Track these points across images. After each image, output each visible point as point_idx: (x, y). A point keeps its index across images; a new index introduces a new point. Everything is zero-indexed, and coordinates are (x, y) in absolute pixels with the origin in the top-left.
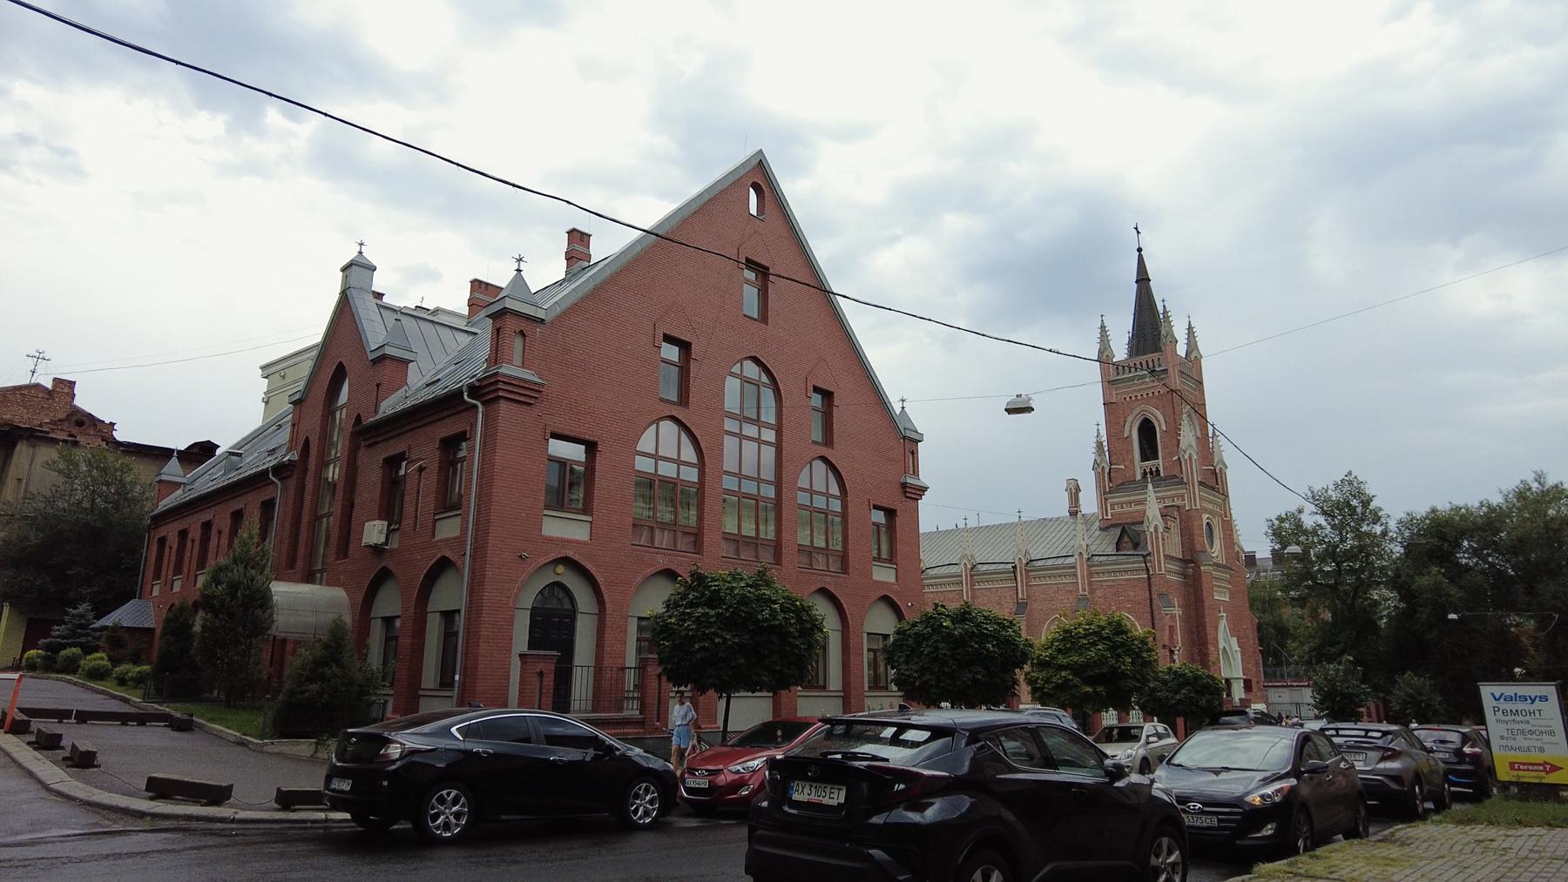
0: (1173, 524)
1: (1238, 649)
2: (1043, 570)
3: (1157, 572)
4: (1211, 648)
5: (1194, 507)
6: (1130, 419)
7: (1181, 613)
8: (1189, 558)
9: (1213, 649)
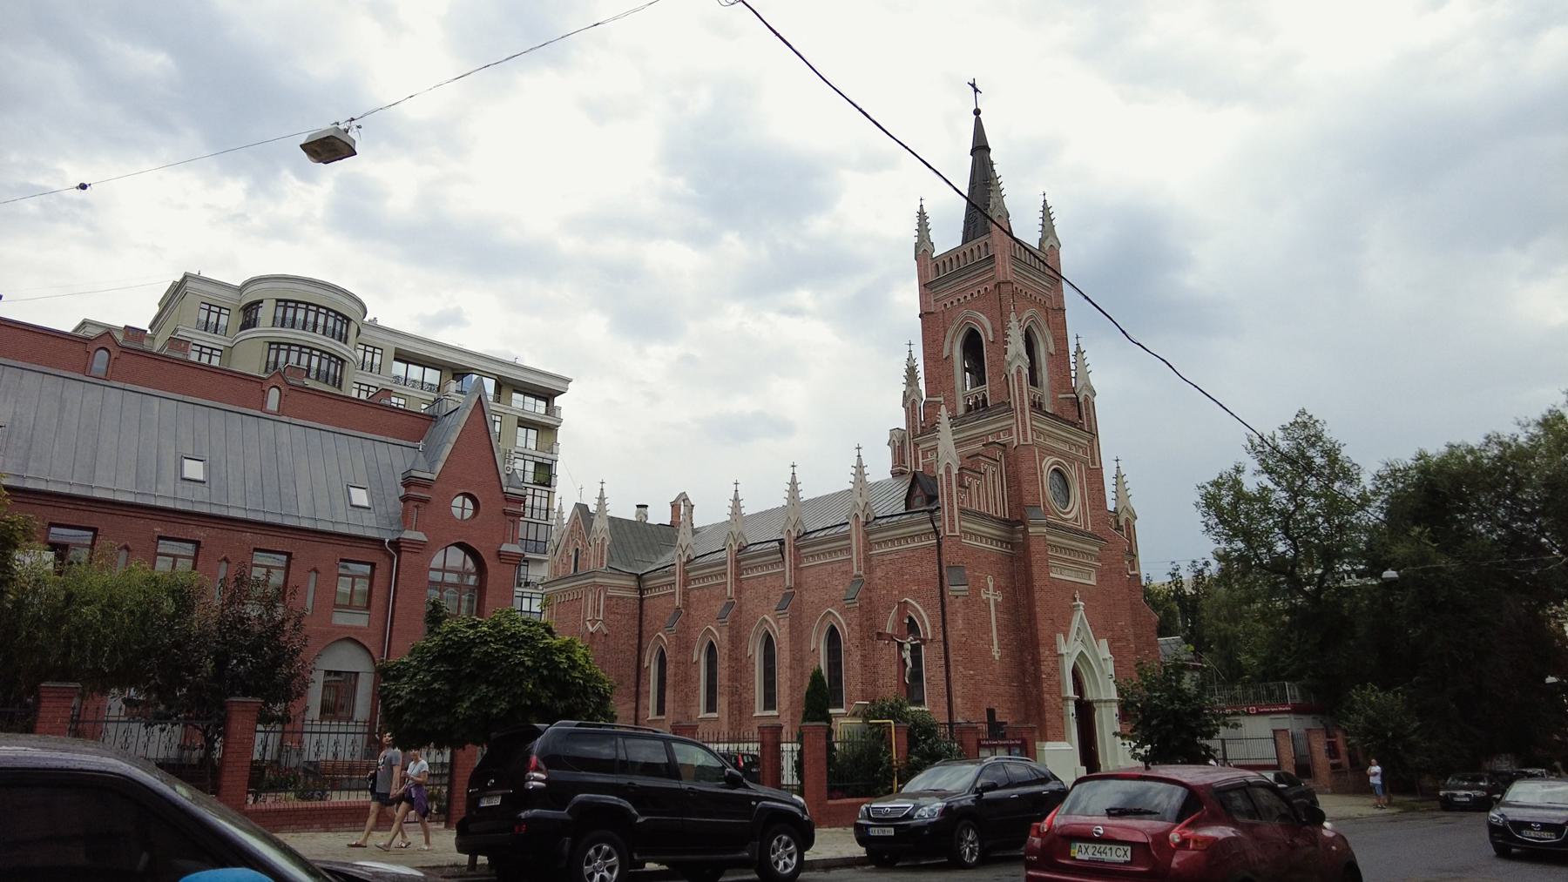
0: (990, 470)
1: (1108, 655)
2: (825, 543)
3: (947, 534)
4: (1045, 652)
5: (1022, 442)
6: (950, 333)
7: (1000, 599)
8: (1019, 518)
9: (1047, 653)
